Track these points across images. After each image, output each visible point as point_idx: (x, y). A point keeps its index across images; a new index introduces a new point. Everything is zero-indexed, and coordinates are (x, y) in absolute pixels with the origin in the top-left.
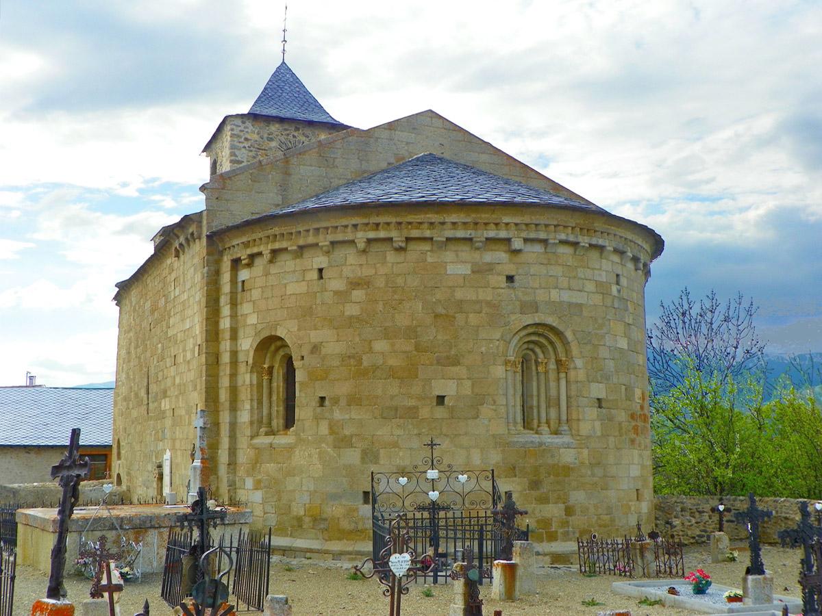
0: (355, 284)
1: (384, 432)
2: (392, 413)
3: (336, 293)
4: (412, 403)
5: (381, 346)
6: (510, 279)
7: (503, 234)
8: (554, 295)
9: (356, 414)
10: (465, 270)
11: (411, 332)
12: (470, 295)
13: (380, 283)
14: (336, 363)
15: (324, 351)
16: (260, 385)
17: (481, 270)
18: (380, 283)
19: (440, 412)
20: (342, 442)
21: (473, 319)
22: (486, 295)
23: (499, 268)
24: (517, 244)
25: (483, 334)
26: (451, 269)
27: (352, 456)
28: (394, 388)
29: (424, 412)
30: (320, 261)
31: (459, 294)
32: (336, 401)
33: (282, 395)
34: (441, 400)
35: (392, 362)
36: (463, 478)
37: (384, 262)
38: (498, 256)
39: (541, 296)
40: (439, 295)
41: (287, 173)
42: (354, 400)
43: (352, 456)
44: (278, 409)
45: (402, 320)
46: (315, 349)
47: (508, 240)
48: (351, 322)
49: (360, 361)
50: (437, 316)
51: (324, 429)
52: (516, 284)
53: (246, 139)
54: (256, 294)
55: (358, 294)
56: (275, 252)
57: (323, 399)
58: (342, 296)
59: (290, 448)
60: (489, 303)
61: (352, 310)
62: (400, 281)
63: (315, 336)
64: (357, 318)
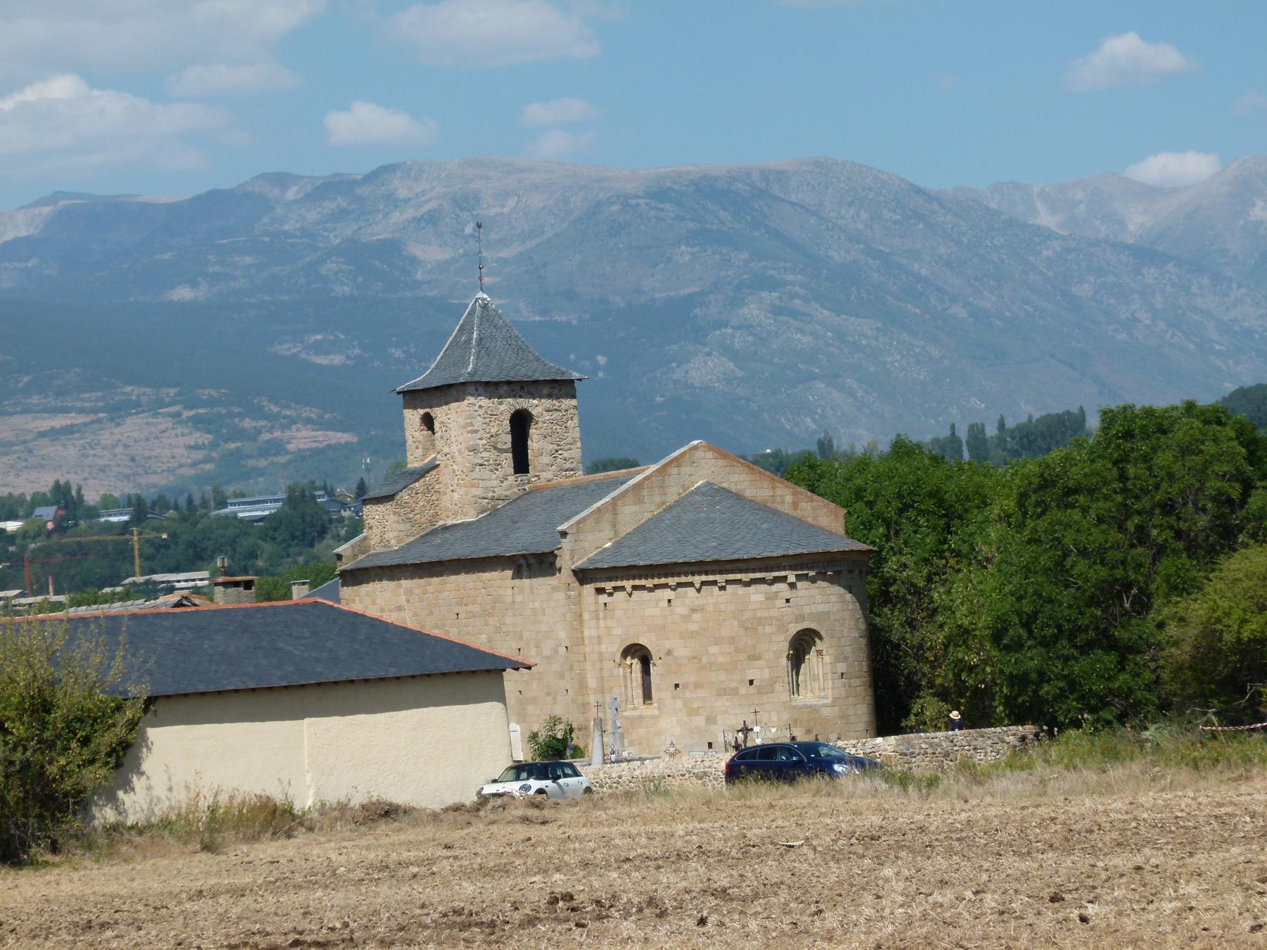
0: (694, 610)
1: (722, 703)
2: (723, 692)
3: (683, 616)
4: (734, 685)
5: (713, 650)
6: (788, 601)
7: (783, 573)
8: (814, 609)
9: (701, 693)
10: (761, 597)
11: (732, 640)
12: (765, 614)
13: (710, 608)
14: (685, 661)
15: (676, 654)
16: (625, 676)
17: (771, 598)
18: (710, 608)
19: (752, 689)
20: (693, 712)
21: (768, 629)
22: (774, 613)
23: (780, 595)
24: (792, 579)
25: (775, 638)
26: (754, 598)
27: (700, 721)
28: (723, 676)
29: (743, 691)
30: (668, 593)
31: (759, 614)
32: (686, 687)
33: (640, 682)
34: (751, 682)
35: (721, 659)
36: (774, 730)
37: (712, 595)
38: (781, 586)
39: (806, 610)
40: (747, 615)
41: (615, 514)
42: (698, 686)
43: (700, 721)
44: (638, 692)
45: (725, 632)
46: (669, 653)
47: (786, 577)
48: (692, 635)
49: (700, 660)
50: (746, 628)
51: (679, 704)
52: (791, 604)
53: (480, 407)
54: (618, 614)
55: (696, 617)
56: (635, 588)
57: (677, 686)
58: (686, 618)
59: (655, 718)
60: (778, 620)
61: (693, 627)
62: (722, 607)
63: (668, 644)
64: (697, 632)
